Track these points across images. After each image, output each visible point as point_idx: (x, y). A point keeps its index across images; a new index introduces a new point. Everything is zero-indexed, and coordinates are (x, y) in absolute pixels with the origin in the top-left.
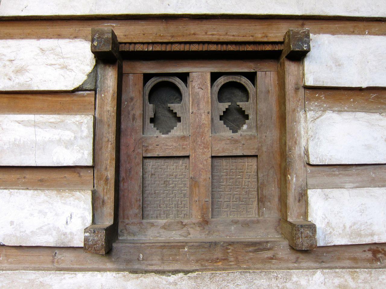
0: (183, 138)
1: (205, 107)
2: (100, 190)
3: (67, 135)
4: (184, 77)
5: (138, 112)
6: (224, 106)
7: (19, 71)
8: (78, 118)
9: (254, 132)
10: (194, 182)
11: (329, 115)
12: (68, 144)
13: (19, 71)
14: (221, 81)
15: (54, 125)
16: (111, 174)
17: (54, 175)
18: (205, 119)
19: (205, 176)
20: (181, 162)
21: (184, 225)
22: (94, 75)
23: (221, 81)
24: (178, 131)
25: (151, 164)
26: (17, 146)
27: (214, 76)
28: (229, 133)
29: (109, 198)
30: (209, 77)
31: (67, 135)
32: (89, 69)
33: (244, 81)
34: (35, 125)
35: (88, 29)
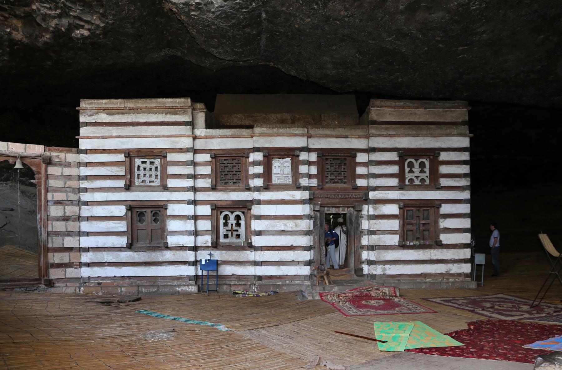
0: (145, 225)
1: (150, 218)
2: (129, 237)
3: (122, 225)
4: (145, 211)
5: (136, 220)
6: (154, 218)
7: (112, 212)
8: (124, 222)
9: (160, 224)
10: (148, 234)
11: (172, 221)
12: (122, 227)
13: (112, 212)
14: (153, 212)
15: (119, 223)
16: (130, 233)
17: (120, 233)
18: (150, 221)
19: (150, 233)
20: (145, 230)
21: (146, 244)
22: (126, 213)
23: (153, 212)
24: (144, 224)
25: (139, 231)
26: (112, 228)
27: (152, 212)
28: (155, 224)
29: (130, 238)
30: (150, 212)
31: (122, 225)
32: (125, 212)
33: (158, 212)
34: (115, 223)
35: (125, 203)
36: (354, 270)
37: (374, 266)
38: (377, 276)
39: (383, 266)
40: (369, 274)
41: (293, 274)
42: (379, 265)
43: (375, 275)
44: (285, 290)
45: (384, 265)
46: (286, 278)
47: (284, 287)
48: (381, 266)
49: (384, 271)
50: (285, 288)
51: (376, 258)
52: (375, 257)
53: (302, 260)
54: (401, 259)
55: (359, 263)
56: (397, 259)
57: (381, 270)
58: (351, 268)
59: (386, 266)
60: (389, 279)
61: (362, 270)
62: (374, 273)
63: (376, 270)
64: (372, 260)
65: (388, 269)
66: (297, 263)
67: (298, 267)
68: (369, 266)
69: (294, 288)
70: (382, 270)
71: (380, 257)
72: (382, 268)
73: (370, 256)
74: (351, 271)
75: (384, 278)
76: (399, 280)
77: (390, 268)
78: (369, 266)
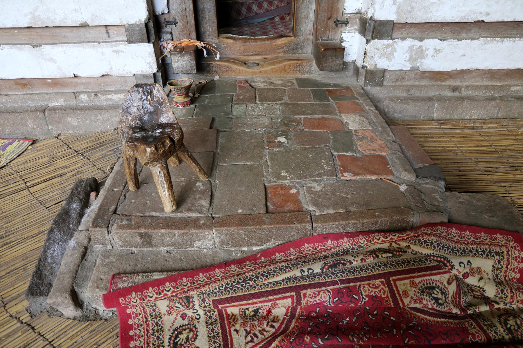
36: (310, 43)
37: (385, 42)
38: (387, 75)
39: (417, 43)
40: (363, 67)
41: (98, 73)
42: (404, 39)
43: (384, 71)
44: (74, 127)
45: (421, 40)
46: (77, 84)
47: (69, 119)
48: (409, 42)
49: (416, 59)
50: (75, 123)
51: (397, 12)
52: (395, 8)
53: (118, 23)
54: (487, 19)
55: (331, 23)
56: (472, 18)
57: (407, 56)
58: (301, 39)
59: (425, 41)
60: (424, 82)
61: (340, 50)
62: (382, 64)
63: (389, 57)
64: (383, 18)
65: (430, 53)
66: (105, 35)
67: (107, 49)
68: (368, 41)
69: (103, 122)
70: (411, 57)
71: (412, 8)
72: (411, 48)
73: (377, 6)
74: (302, 47)
75: (410, 79)
76: (455, 89)
77: (437, 51)
78: (368, 41)
